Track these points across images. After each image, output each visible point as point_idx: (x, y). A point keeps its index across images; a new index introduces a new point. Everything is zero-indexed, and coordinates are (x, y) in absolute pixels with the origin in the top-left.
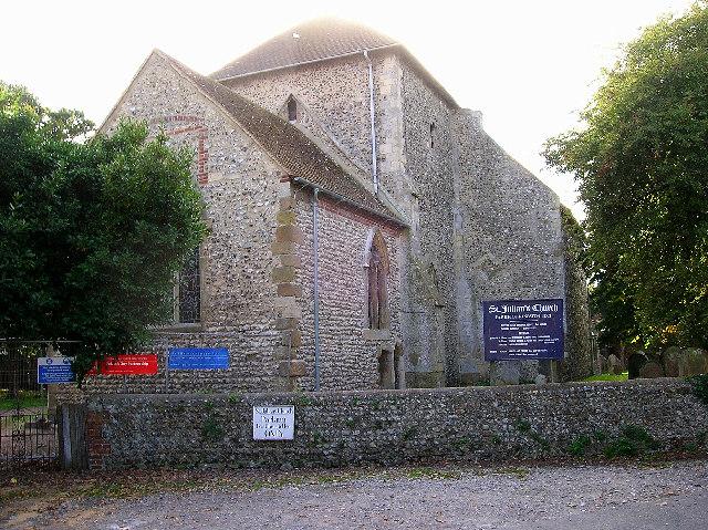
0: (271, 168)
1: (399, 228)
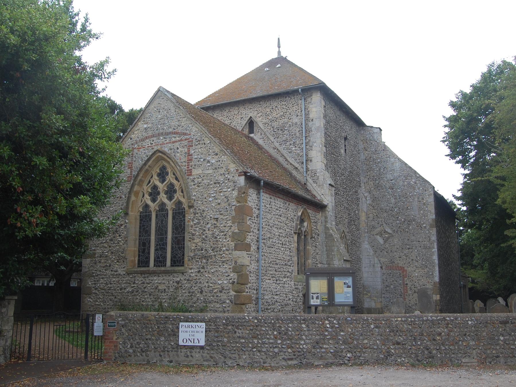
0: (232, 167)
1: (320, 207)
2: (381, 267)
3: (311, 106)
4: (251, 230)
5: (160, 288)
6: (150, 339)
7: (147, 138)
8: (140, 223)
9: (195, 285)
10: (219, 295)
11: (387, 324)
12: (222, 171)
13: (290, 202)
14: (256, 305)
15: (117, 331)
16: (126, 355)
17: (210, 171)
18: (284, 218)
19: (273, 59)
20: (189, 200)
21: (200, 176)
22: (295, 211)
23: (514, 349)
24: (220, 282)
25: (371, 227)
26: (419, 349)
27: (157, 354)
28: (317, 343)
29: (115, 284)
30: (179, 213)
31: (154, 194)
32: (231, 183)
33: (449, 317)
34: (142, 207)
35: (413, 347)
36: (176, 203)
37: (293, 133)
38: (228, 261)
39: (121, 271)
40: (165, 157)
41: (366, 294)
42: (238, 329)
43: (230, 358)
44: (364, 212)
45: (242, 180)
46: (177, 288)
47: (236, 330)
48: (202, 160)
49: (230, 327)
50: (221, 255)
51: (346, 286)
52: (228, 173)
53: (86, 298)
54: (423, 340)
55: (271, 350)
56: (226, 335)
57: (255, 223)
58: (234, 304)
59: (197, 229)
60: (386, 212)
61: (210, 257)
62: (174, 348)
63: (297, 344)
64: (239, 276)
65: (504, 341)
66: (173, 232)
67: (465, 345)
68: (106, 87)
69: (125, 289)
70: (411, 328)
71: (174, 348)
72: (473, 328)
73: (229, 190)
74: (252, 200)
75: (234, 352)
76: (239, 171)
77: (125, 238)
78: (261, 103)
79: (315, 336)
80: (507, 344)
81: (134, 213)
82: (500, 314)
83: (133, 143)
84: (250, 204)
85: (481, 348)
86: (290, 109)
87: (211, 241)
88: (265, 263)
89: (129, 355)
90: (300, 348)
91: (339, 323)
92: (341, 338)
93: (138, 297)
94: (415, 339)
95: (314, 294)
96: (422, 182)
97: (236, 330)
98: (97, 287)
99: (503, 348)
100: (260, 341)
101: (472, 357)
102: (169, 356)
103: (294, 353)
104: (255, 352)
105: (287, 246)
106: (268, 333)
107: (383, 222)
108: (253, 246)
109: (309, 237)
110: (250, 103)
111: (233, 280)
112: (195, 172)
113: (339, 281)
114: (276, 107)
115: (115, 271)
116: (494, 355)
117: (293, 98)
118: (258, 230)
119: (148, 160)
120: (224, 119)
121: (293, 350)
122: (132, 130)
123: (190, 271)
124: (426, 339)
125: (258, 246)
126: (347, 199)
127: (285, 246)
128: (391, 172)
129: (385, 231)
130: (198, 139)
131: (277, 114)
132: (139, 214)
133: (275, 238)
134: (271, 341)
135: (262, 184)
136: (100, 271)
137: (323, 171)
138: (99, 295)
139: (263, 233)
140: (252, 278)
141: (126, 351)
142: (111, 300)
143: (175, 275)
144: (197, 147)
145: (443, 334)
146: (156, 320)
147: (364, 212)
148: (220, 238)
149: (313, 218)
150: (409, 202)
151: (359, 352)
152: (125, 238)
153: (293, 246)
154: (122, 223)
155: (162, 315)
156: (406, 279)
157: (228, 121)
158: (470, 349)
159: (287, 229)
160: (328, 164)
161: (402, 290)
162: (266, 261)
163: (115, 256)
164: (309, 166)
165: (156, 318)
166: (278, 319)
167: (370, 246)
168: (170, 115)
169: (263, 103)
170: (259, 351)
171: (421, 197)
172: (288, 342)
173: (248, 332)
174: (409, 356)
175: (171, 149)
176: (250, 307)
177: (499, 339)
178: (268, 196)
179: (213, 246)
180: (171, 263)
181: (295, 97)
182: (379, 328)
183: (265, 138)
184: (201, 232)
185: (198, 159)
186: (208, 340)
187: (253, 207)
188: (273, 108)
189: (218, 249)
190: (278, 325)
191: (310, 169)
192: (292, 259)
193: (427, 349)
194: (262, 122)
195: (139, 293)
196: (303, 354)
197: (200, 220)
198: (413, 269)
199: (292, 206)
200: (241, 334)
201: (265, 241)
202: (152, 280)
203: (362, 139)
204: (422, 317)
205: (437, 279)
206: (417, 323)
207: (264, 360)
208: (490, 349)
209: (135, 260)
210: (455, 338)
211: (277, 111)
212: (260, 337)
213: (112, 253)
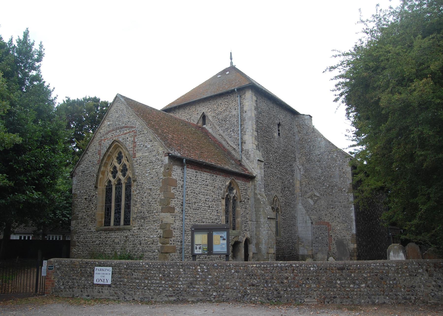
0: (161, 150)
1: (250, 178)
2: (312, 223)
3: (245, 101)
4: (175, 197)
5: (116, 241)
7: (109, 132)
8: (106, 194)
9: (136, 239)
10: (151, 246)
11: (244, 270)
12: (154, 153)
15: (54, 273)
16: (59, 290)
17: (147, 154)
18: (211, 187)
20: (133, 176)
21: (140, 158)
22: (223, 182)
23: (349, 291)
24: (152, 236)
26: (270, 290)
27: (80, 290)
28: (191, 284)
29: (89, 238)
31: (114, 173)
32: (160, 162)
33: (295, 264)
35: (265, 288)
36: (128, 179)
37: (232, 123)
38: (157, 220)
39: (93, 229)
40: (120, 145)
42: (135, 272)
43: (129, 294)
44: (299, 181)
45: (166, 159)
46: (125, 241)
47: (133, 273)
48: (142, 146)
49: (129, 271)
50: (153, 216)
51: (222, 239)
52: (158, 155)
53: (73, 249)
54: (274, 283)
55: (158, 288)
56: (126, 277)
57: (180, 191)
58: (160, 253)
59: (139, 197)
60: (315, 180)
62: (91, 286)
63: (177, 284)
65: (341, 284)
66: (126, 200)
67: (308, 288)
68: (57, 96)
69: (95, 242)
70: (263, 273)
71: (91, 286)
72: (314, 273)
73: (158, 167)
74: (177, 174)
75: (131, 290)
76: (165, 153)
77: (96, 205)
78: (211, 101)
79: (190, 279)
81: (102, 187)
82: (368, 261)
85: (320, 290)
87: (147, 206)
88: (190, 221)
89: (61, 291)
90: (179, 288)
91: (208, 268)
92: (209, 280)
93: (102, 248)
94: (267, 282)
95: (197, 245)
96: (342, 156)
97: (133, 273)
98: (79, 241)
99: (339, 291)
100: (150, 282)
101: (313, 297)
102: (87, 292)
103: (174, 291)
104: (146, 290)
105: (214, 209)
106: (156, 275)
107: (313, 188)
108: (178, 209)
109: (238, 201)
110: (203, 102)
111: (160, 235)
112: (138, 155)
113: (217, 235)
114: (221, 104)
115: (89, 229)
116: (332, 296)
117: (232, 96)
118: (183, 197)
120: (186, 115)
121: (173, 289)
123: (134, 229)
124: (276, 281)
125: (182, 208)
126: (281, 171)
127: (212, 208)
128: (318, 149)
129: (315, 194)
130: (140, 130)
131: (221, 109)
132: (105, 187)
133: (201, 203)
134: (158, 282)
135: (184, 161)
136: (81, 229)
137: (253, 150)
138: (80, 247)
139: (188, 199)
140: (176, 233)
141: (59, 287)
142: (87, 250)
143: (125, 231)
144: (139, 136)
145: (289, 278)
146: (80, 265)
147: (299, 181)
148: (152, 204)
149: (243, 186)
150: (333, 171)
151: (223, 291)
152: (96, 205)
153: (220, 208)
154: (94, 194)
155: (84, 261)
156: (330, 232)
157: (189, 117)
158: (311, 291)
159: (214, 196)
160: (260, 145)
162: (191, 220)
163: (89, 218)
164: (243, 147)
165: (79, 263)
166: (163, 265)
167: (303, 207)
168: (123, 114)
169: (212, 101)
170: (149, 289)
171: (341, 167)
172: (170, 283)
173: (141, 274)
174: (261, 295)
175: (123, 139)
176: (174, 255)
177: (336, 283)
178: (193, 170)
179: (148, 210)
180: (124, 223)
181: (234, 95)
182: (238, 272)
185: (140, 145)
186: (114, 280)
188: (218, 105)
189: (151, 212)
190: (162, 269)
191: (245, 149)
192: (219, 218)
193: (277, 290)
194: (211, 115)
195: (103, 245)
196: (181, 292)
198: (336, 224)
200: (137, 276)
201: (190, 205)
202: (111, 235)
203: (297, 124)
204: (273, 264)
205: (354, 232)
206: (268, 268)
207: (152, 296)
208: (328, 291)
209: (102, 221)
210: (300, 281)
211: (222, 106)
212: (149, 278)
213: (88, 216)
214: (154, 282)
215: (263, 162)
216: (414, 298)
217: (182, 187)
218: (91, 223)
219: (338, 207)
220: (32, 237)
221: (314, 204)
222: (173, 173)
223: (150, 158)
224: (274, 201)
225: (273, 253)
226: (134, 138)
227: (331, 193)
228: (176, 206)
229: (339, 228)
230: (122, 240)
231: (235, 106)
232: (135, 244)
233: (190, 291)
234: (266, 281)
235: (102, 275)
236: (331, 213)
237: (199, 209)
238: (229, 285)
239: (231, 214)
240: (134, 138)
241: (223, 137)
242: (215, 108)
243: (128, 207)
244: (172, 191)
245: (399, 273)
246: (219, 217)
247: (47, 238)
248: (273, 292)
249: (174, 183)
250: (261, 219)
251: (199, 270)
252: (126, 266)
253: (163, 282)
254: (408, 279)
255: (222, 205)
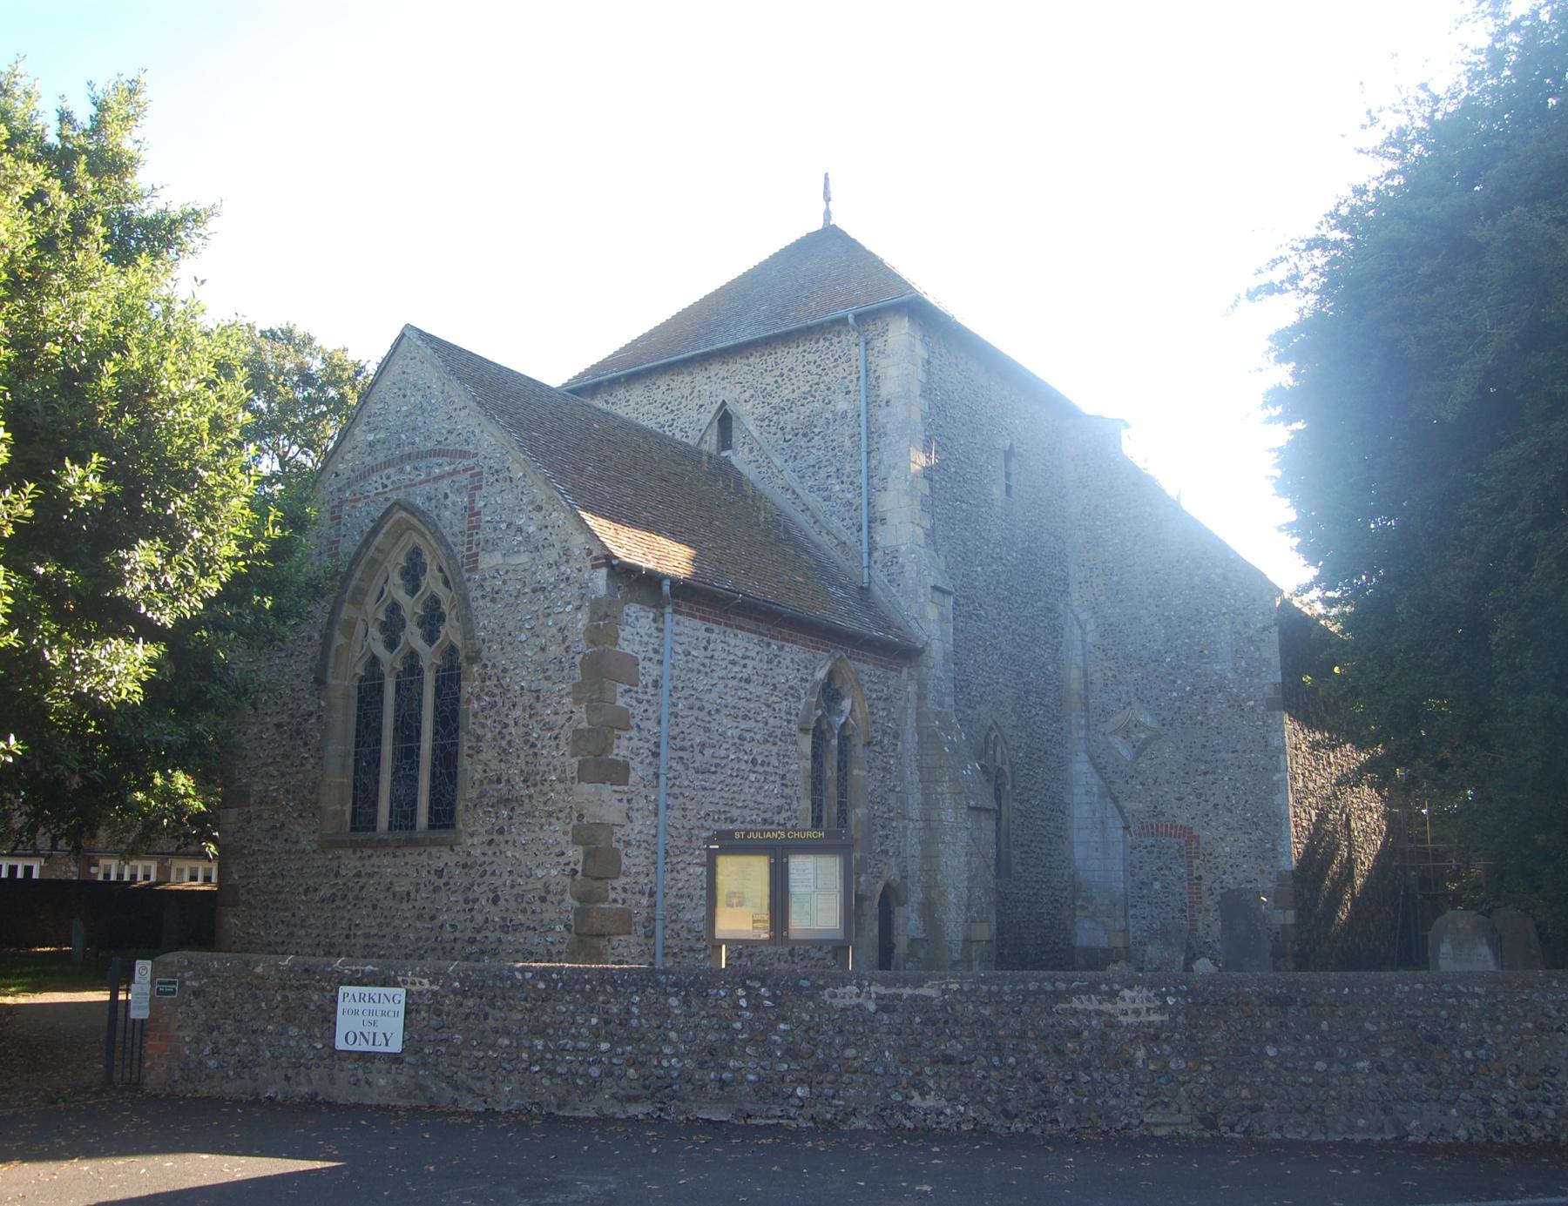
2: (1126, 828)
3: (884, 362)
4: (633, 722)
5: (398, 889)
6: (262, 1031)
7: (373, 470)
8: (359, 709)
9: (481, 880)
10: (538, 910)
12: (552, 555)
13: (784, 639)
14: (647, 937)
17: (523, 559)
18: (760, 689)
19: (809, 235)
21: (497, 571)
22: (806, 668)
24: (540, 873)
25: (1099, 711)
26: (1011, 1078)
30: (451, 678)
31: (392, 629)
34: (363, 661)
37: (834, 444)
38: (561, 811)
40: (415, 521)
41: (1083, 908)
42: (493, 1005)
43: (470, 1090)
47: (487, 1009)
49: (471, 1003)
50: (546, 794)
54: (1026, 1053)
57: (648, 701)
60: (1140, 665)
61: (519, 800)
64: (588, 855)
66: (436, 732)
67: (1155, 1071)
69: (316, 890)
71: (322, 1059)
73: (569, 608)
75: (481, 1074)
76: (594, 554)
78: (752, 360)
79: (706, 1034)
80: (1286, 1069)
83: (340, 485)
84: (627, 648)
85: (1202, 1080)
86: (827, 374)
87: (522, 756)
88: (684, 817)
89: (208, 1076)
90: (662, 1068)
91: (774, 994)
93: (345, 914)
97: (487, 1009)
98: (251, 886)
101: (1174, 1106)
103: (646, 1079)
104: (537, 1076)
105: (770, 769)
108: (639, 768)
109: (858, 742)
111: (572, 866)
112: (489, 561)
114: (791, 370)
116: (1245, 1103)
117: (835, 340)
119: (375, 531)
120: (655, 411)
122: (339, 451)
123: (469, 842)
127: (766, 768)
131: (793, 391)
134: (582, 1045)
135: (666, 588)
139: (677, 730)
140: (633, 860)
141: (201, 1063)
142: (283, 922)
143: (434, 850)
145: (1086, 1033)
148: (543, 747)
149: (876, 687)
152: (318, 750)
153: (794, 767)
154: (312, 709)
157: (667, 418)
159: (771, 721)
161: (1186, 895)
163: (294, 799)
164: (878, 539)
166: (602, 982)
168: (430, 404)
169: (758, 360)
170: (552, 1073)
173: (519, 1016)
174: (978, 1098)
176: (623, 944)
177: (1262, 1054)
178: (697, 623)
180: (430, 820)
181: (843, 337)
183: (761, 460)
184: (497, 730)
187: (640, 657)
188: (782, 375)
189: (538, 778)
190: (601, 999)
193: (1037, 1080)
197: (493, 695)
199: (794, 653)
200: (500, 1021)
202: (379, 867)
208: (1231, 1084)
211: (794, 381)
212: (551, 1031)
214: (568, 1047)
215: (950, 593)
216: (1551, 1114)
217: (656, 684)
218: (300, 820)
219: (1226, 768)
220: (42, 868)
221: (1137, 758)
222: (623, 630)
223: (534, 573)
224: (986, 743)
225: (988, 942)
226: (472, 496)
227: (1199, 718)
228: (633, 757)
229: (1227, 849)
230: (422, 886)
231: (847, 380)
232: (475, 900)
233: (707, 1081)
234: (997, 1044)
235: (368, 1018)
236: (1201, 791)
237: (719, 770)
238: (855, 1059)
239: (832, 790)
240: (472, 496)
241: (798, 497)
242: (769, 388)
243: (447, 760)
244: (620, 702)
245: (1498, 1019)
246: (789, 801)
247: (96, 874)
248: (1025, 1088)
249: (628, 670)
250: (944, 810)
251: (743, 1003)
252: (460, 983)
253: (604, 1046)
254: (1531, 1041)
255: (802, 756)
